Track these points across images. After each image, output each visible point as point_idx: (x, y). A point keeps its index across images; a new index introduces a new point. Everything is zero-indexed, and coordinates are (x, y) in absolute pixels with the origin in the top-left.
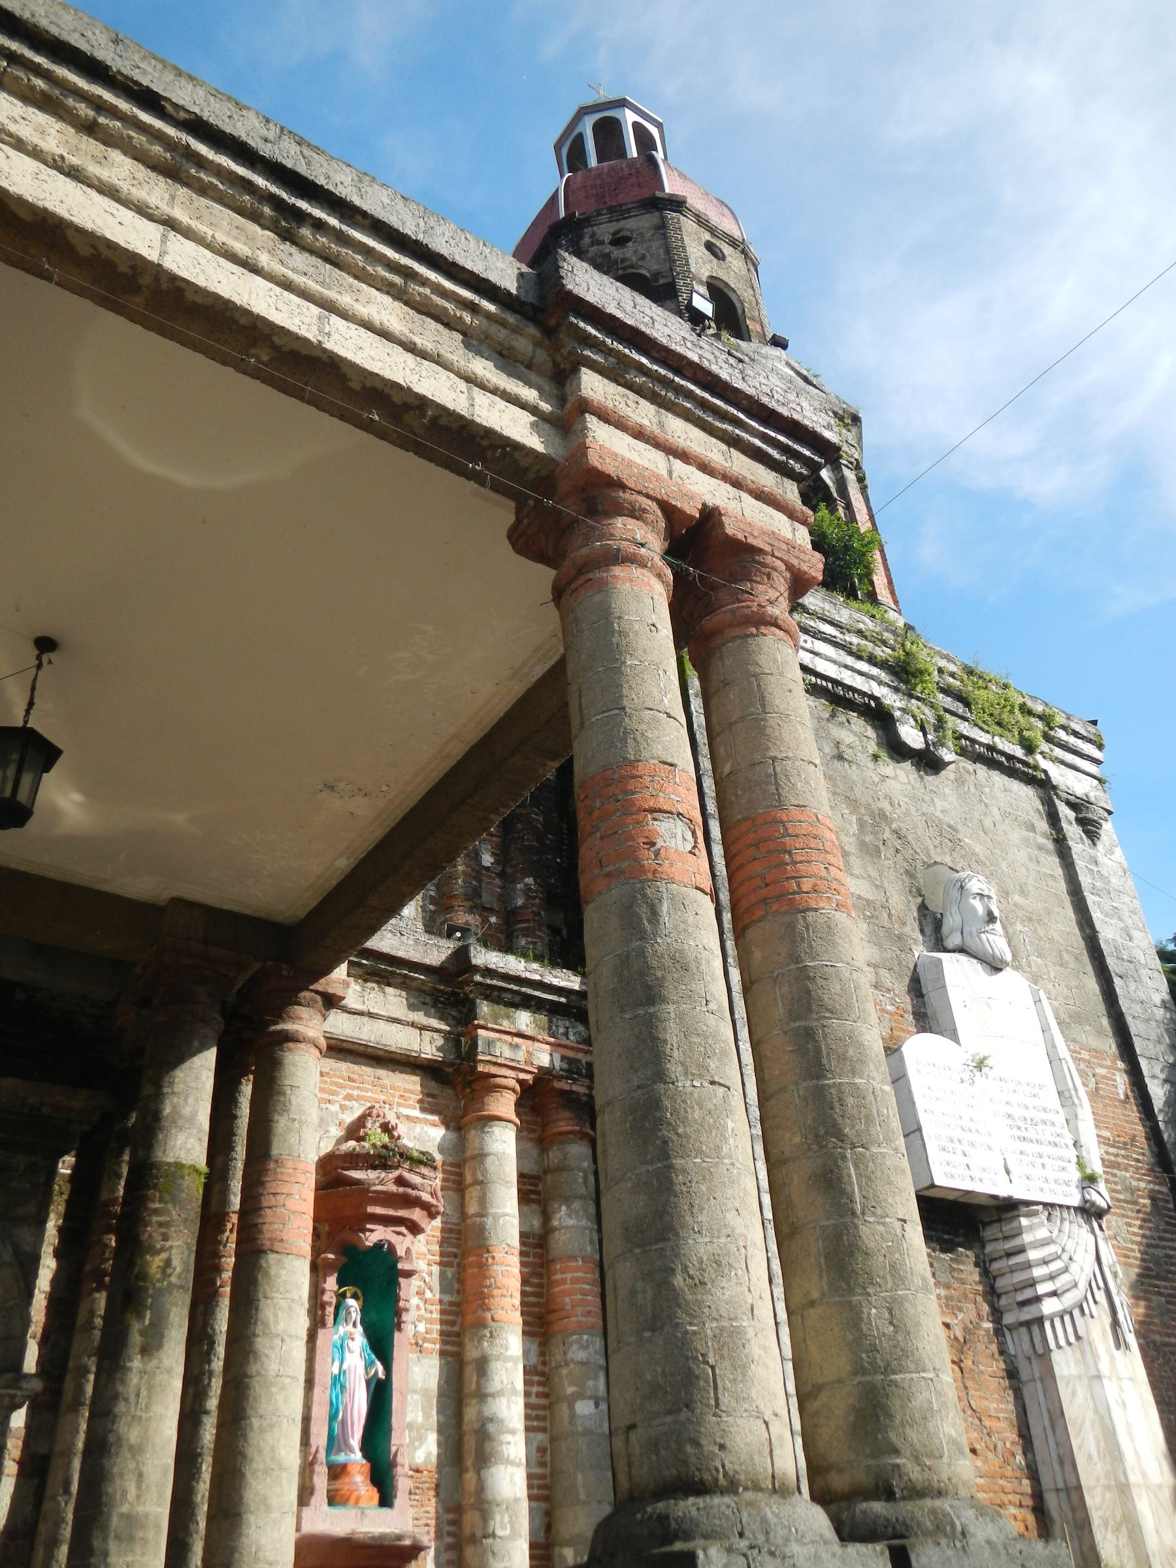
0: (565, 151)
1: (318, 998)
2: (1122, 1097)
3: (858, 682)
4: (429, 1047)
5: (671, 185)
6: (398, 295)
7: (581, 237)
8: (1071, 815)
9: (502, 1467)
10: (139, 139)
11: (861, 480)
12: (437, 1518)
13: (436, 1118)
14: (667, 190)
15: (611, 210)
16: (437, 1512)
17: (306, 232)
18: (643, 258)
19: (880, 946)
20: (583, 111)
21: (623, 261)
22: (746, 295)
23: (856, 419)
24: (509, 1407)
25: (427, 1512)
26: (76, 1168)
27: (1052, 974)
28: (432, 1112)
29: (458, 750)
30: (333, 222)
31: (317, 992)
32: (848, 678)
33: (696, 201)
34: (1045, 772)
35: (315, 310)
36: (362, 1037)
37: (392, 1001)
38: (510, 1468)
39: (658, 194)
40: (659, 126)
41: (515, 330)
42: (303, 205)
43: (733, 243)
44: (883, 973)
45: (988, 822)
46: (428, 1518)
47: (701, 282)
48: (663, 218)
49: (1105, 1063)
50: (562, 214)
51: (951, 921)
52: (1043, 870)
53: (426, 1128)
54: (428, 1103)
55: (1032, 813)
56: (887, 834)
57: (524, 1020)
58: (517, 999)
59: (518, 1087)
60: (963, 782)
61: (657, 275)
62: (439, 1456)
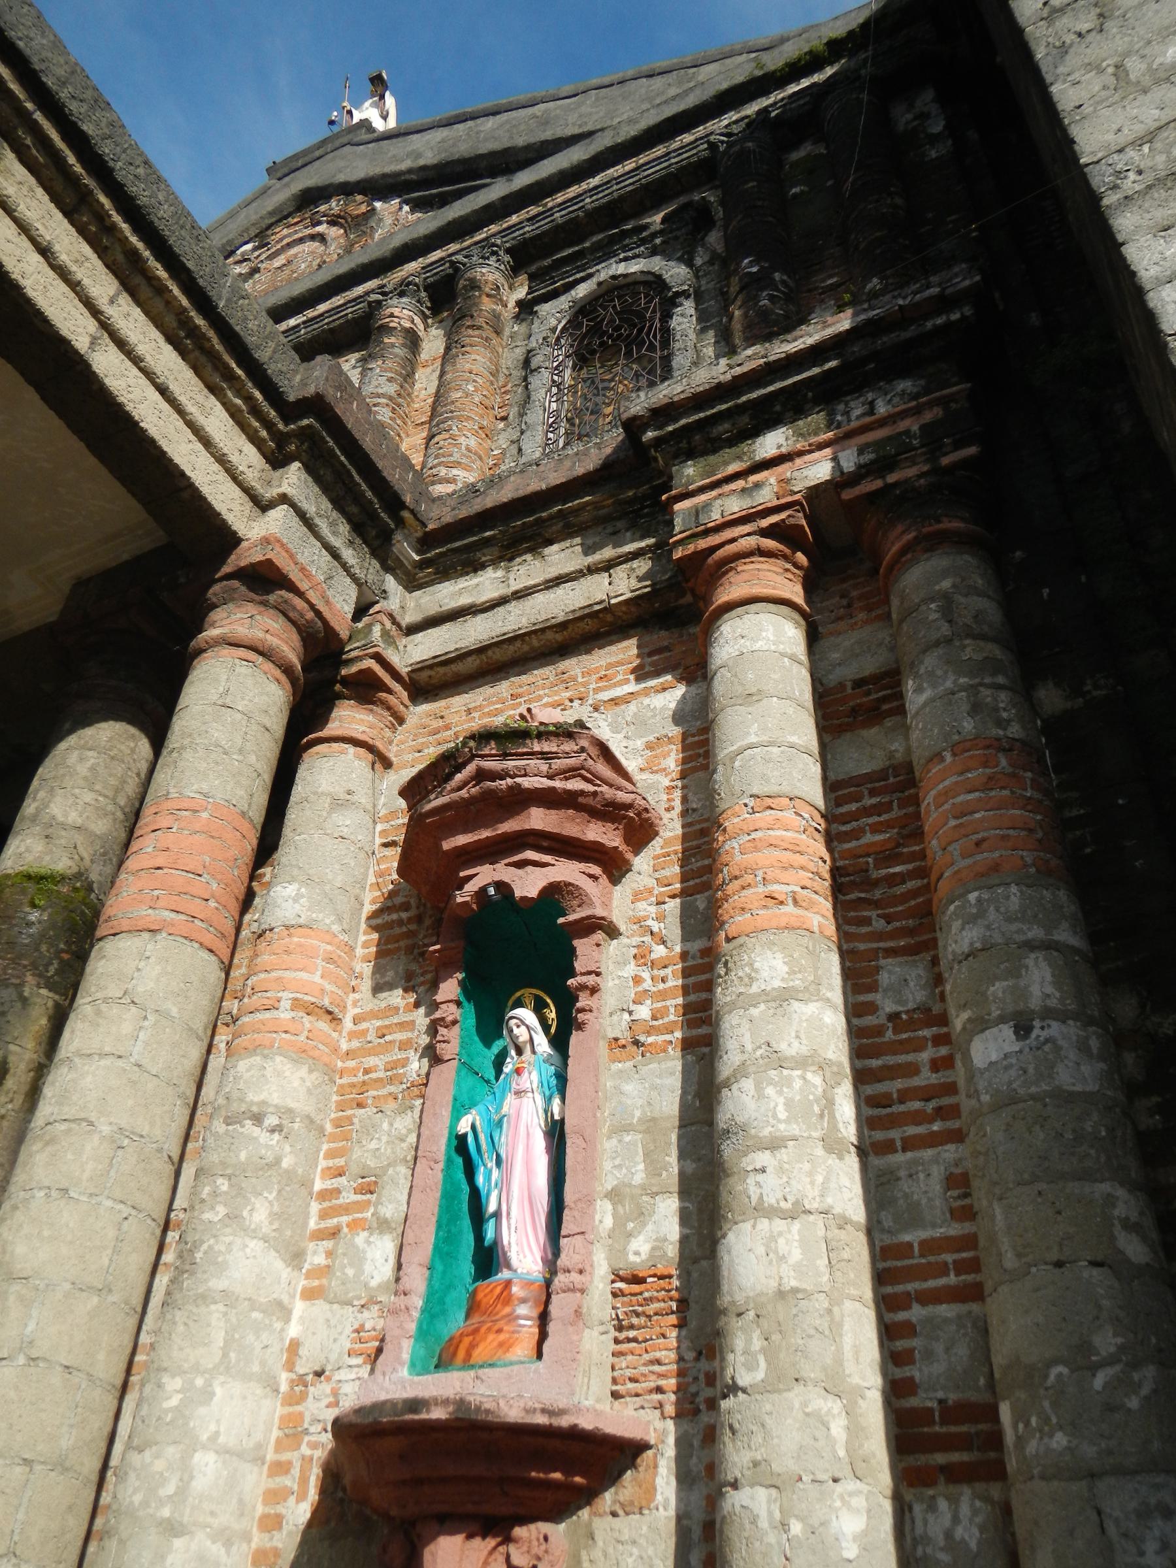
1: (235, 583)
4: (622, 585)
9: (746, 1226)
12: (681, 1374)
13: (669, 677)
16: (681, 1359)
24: (760, 1095)
25: (658, 1362)
28: (657, 674)
31: (228, 577)
36: (505, 630)
37: (563, 556)
38: (763, 1224)
46: (661, 1376)
53: (646, 701)
54: (652, 664)
57: (771, 443)
58: (745, 420)
59: (769, 544)
62: (684, 1240)
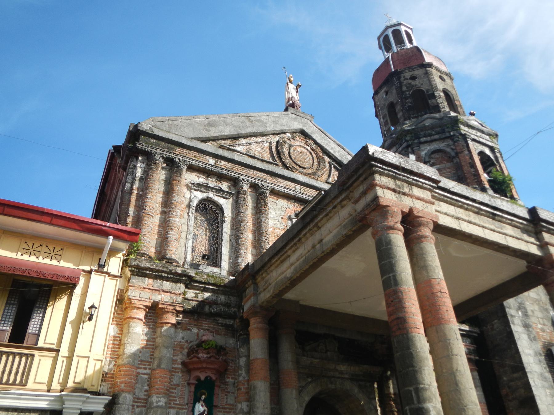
0: (381, 39)
5: (428, 59)
6: (510, 224)
7: (400, 77)
10: (473, 208)
11: (501, 155)
15: (409, 68)
17: (496, 218)
18: (422, 84)
19: (542, 312)
20: (387, 28)
21: (416, 85)
22: (453, 92)
23: (497, 136)
26: (378, 385)
29: (479, 292)
30: (500, 214)
33: (435, 63)
35: (504, 236)
39: (424, 63)
40: (411, 29)
41: (529, 226)
42: (496, 212)
43: (448, 75)
44: (545, 321)
48: (426, 70)
50: (393, 70)
61: (428, 91)
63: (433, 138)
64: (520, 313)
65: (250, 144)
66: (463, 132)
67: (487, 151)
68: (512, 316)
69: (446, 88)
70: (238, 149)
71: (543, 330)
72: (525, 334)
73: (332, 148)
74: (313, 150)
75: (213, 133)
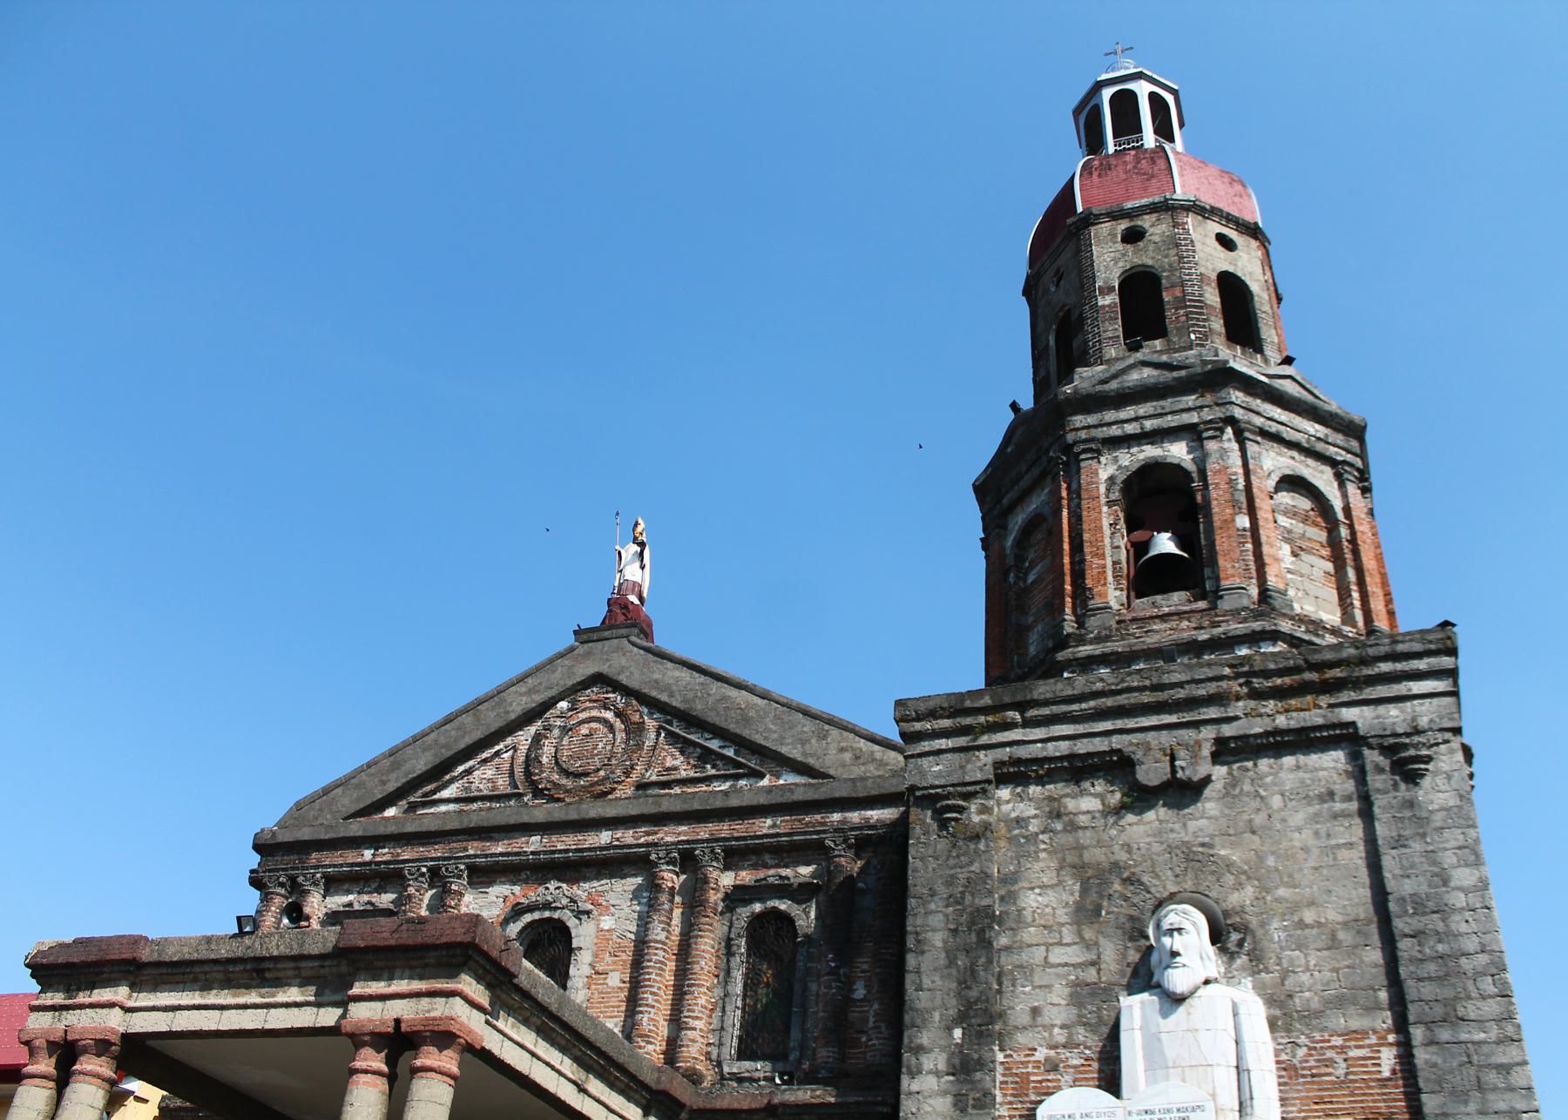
2: (1386, 1074)
3: (1100, 745)
8: (1384, 762)
14: (1080, 209)
20: (1077, 112)
27: (1312, 963)
32: (1083, 747)
34: (1353, 724)
39: (1070, 221)
40: (1139, 76)
43: (1154, 208)
44: (1081, 1030)
45: (1259, 819)
47: (1111, 289)
49: (1367, 1042)
51: (1155, 958)
52: (1333, 842)
55: (1335, 777)
56: (1117, 886)
60: (1234, 786)
63: (1024, 484)
64: (958, 1033)
65: (469, 772)
66: (1070, 437)
67: (1178, 451)
68: (919, 1050)
69: (1137, 261)
70: (445, 794)
71: (1052, 1066)
72: (945, 1093)
73: (667, 688)
74: (618, 714)
75: (392, 786)
